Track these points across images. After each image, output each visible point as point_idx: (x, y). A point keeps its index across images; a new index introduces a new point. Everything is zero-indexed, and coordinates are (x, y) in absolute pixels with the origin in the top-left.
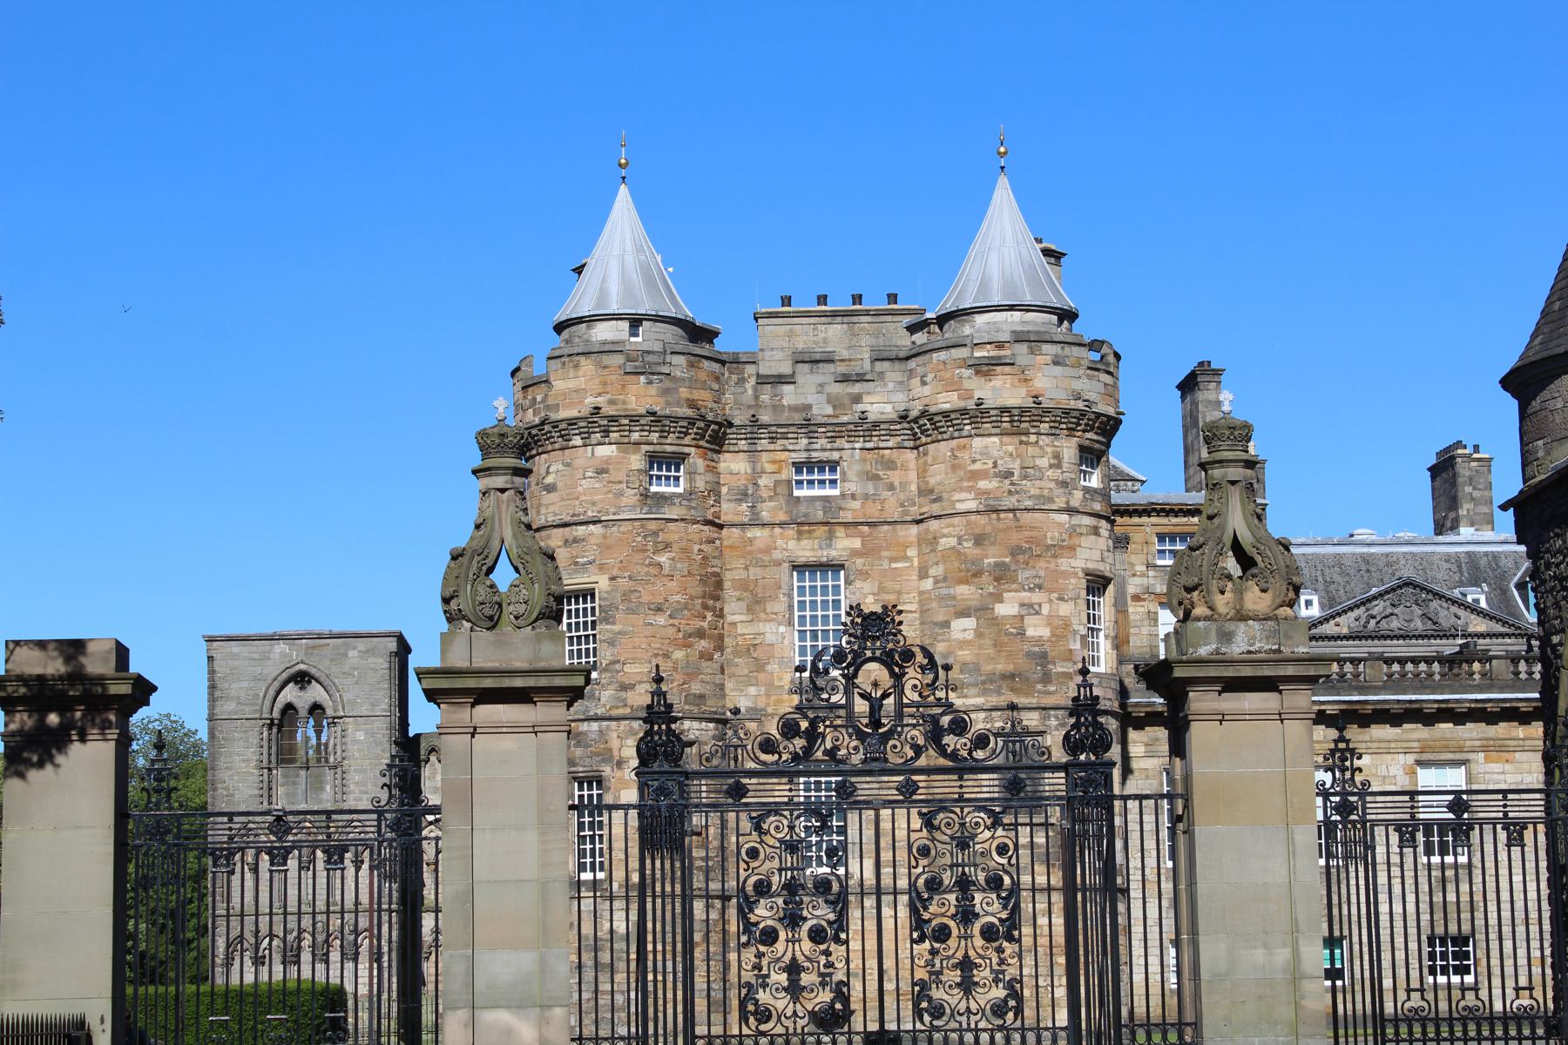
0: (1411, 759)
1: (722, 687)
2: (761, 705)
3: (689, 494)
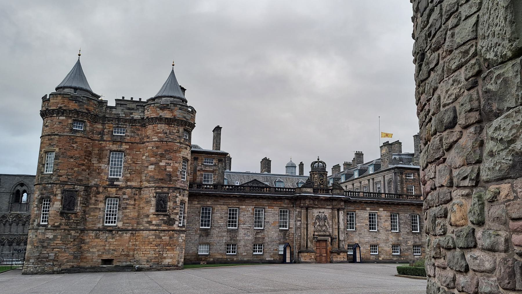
0: (253, 207)
1: (88, 178)
2: (98, 183)
3: (84, 131)
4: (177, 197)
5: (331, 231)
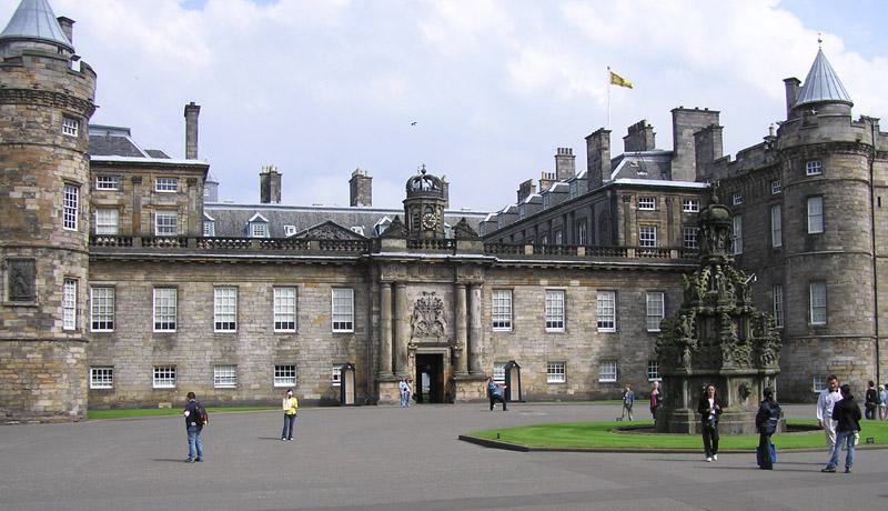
0: (271, 285)
4: (54, 267)
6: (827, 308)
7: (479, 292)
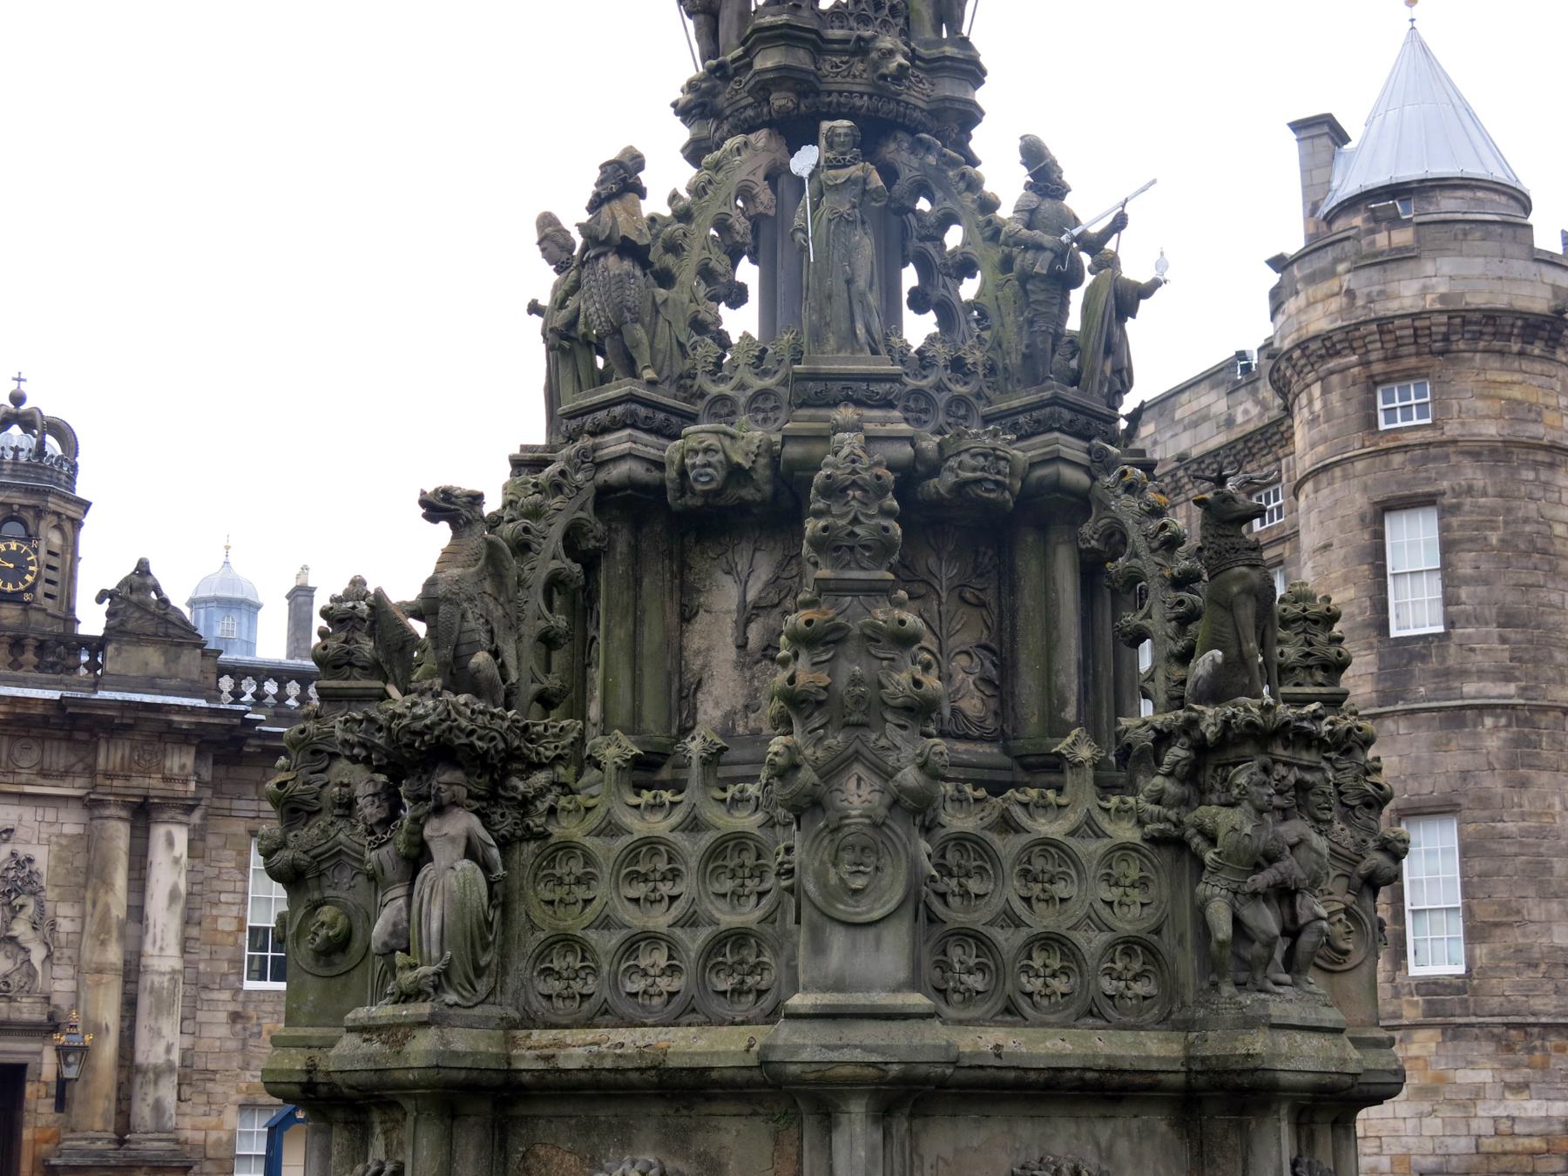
5: (62, 986)
6: (1468, 911)
7: (181, 836)
